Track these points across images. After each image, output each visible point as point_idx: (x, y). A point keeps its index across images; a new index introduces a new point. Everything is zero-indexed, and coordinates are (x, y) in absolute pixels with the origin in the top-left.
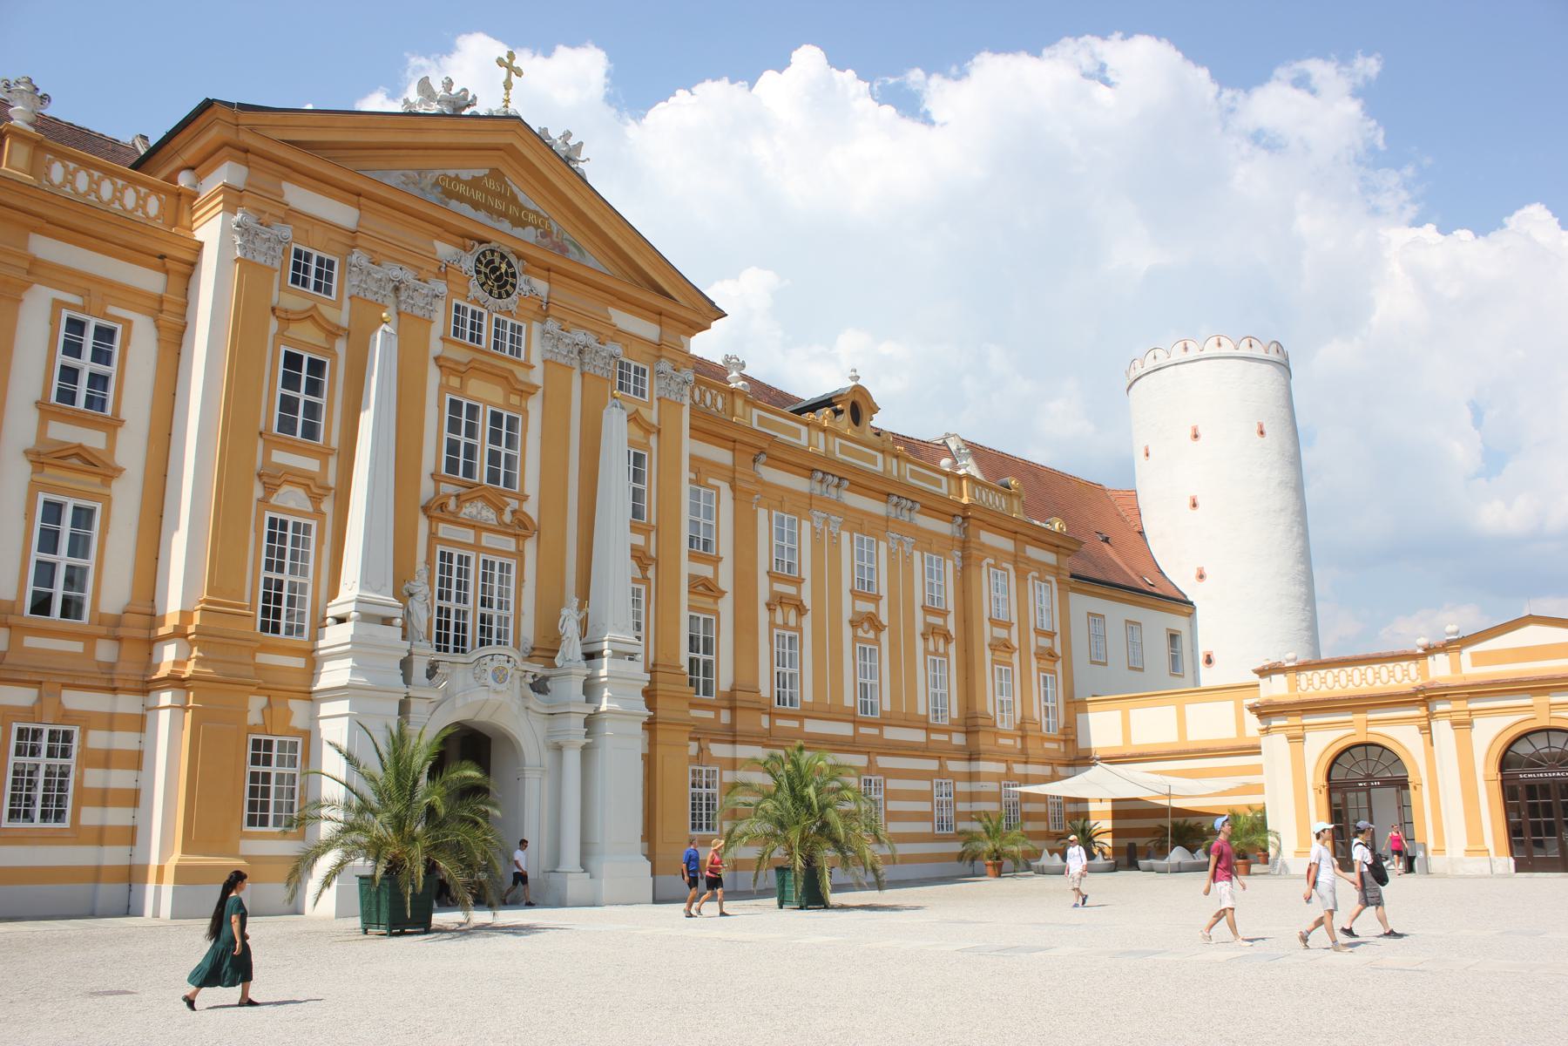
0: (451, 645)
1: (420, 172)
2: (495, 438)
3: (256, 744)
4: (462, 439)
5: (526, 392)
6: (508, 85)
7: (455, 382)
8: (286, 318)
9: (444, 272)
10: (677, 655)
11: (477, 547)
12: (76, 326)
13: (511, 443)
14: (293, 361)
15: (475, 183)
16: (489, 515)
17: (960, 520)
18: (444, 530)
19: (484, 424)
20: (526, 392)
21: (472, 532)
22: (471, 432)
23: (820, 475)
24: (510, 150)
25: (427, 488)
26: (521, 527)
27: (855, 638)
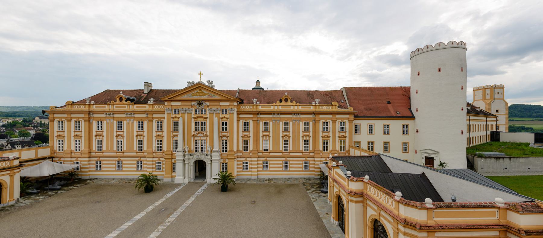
0: (197, 151)
1: (189, 94)
2: (202, 125)
3: (174, 164)
4: (197, 126)
5: (206, 118)
6: (200, 77)
7: (196, 119)
8: (173, 118)
9: (192, 106)
10: (233, 148)
11: (200, 139)
12: (158, 122)
13: (205, 125)
14: (175, 122)
15: (197, 92)
16: (202, 135)
17: (313, 114)
18: (195, 138)
19: (200, 124)
20: (206, 118)
21: (199, 137)
22: (199, 125)
23: (273, 114)
24: (200, 86)
25: (193, 133)
26: (206, 136)
27: (283, 139)
